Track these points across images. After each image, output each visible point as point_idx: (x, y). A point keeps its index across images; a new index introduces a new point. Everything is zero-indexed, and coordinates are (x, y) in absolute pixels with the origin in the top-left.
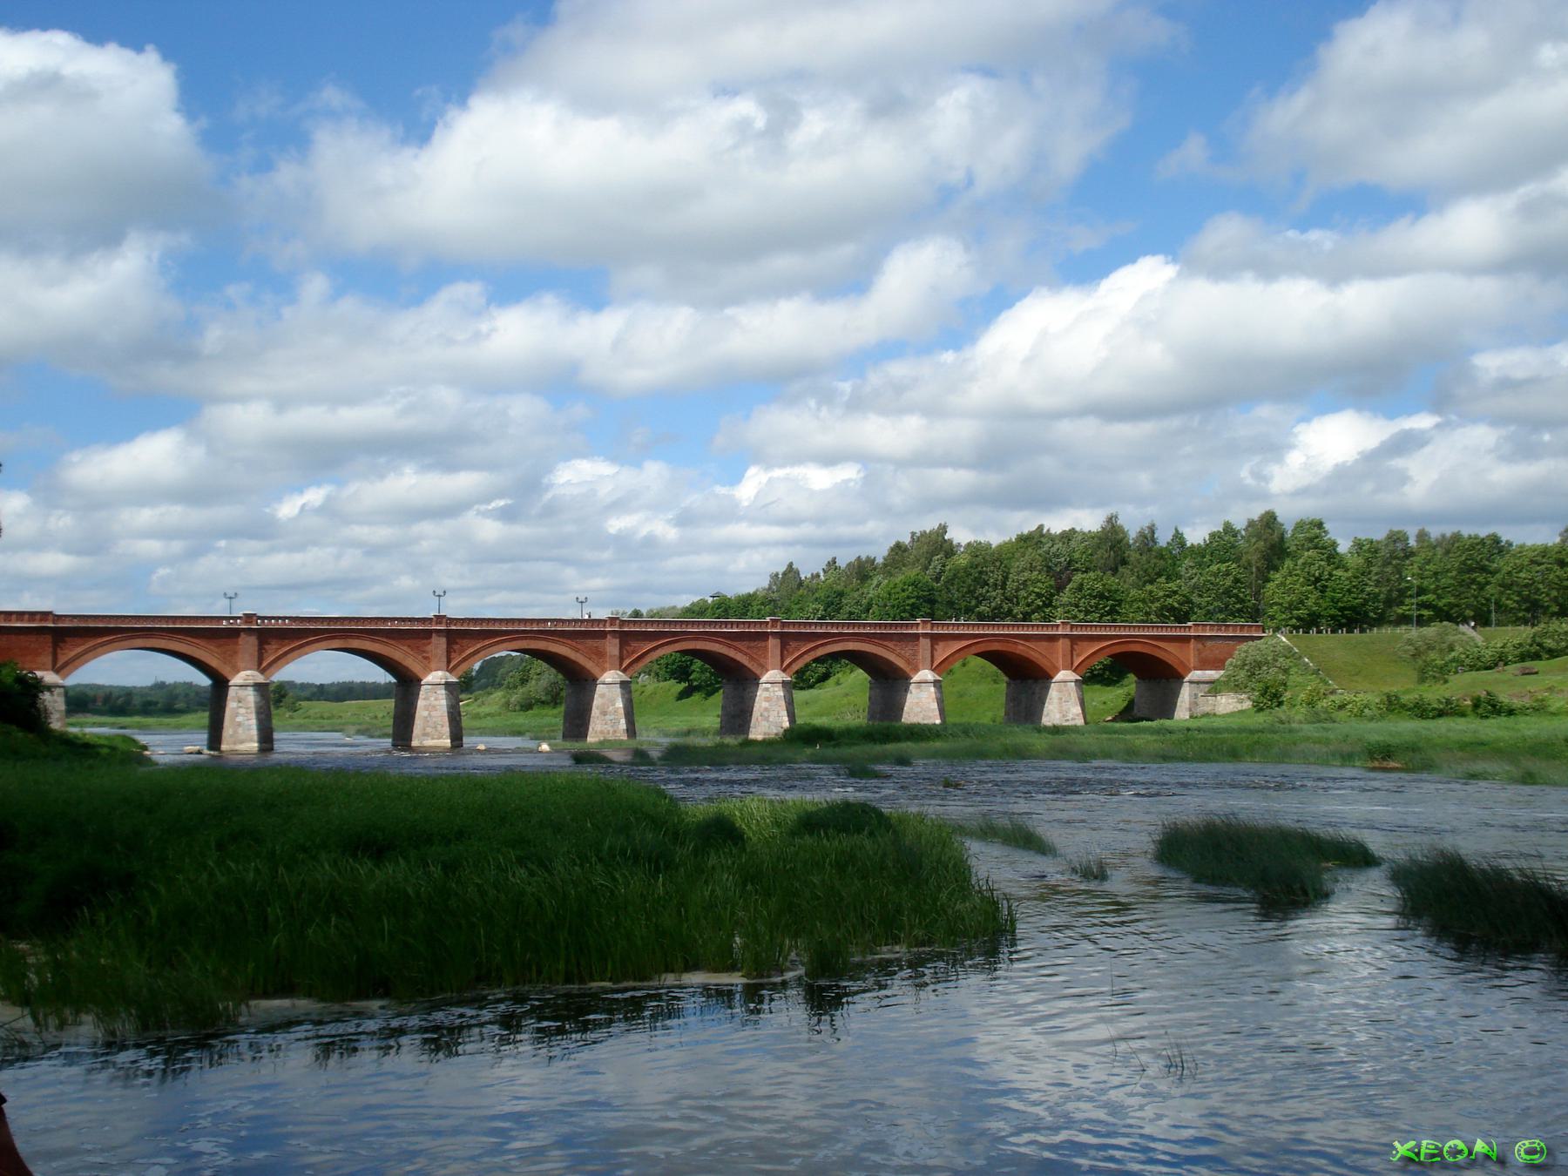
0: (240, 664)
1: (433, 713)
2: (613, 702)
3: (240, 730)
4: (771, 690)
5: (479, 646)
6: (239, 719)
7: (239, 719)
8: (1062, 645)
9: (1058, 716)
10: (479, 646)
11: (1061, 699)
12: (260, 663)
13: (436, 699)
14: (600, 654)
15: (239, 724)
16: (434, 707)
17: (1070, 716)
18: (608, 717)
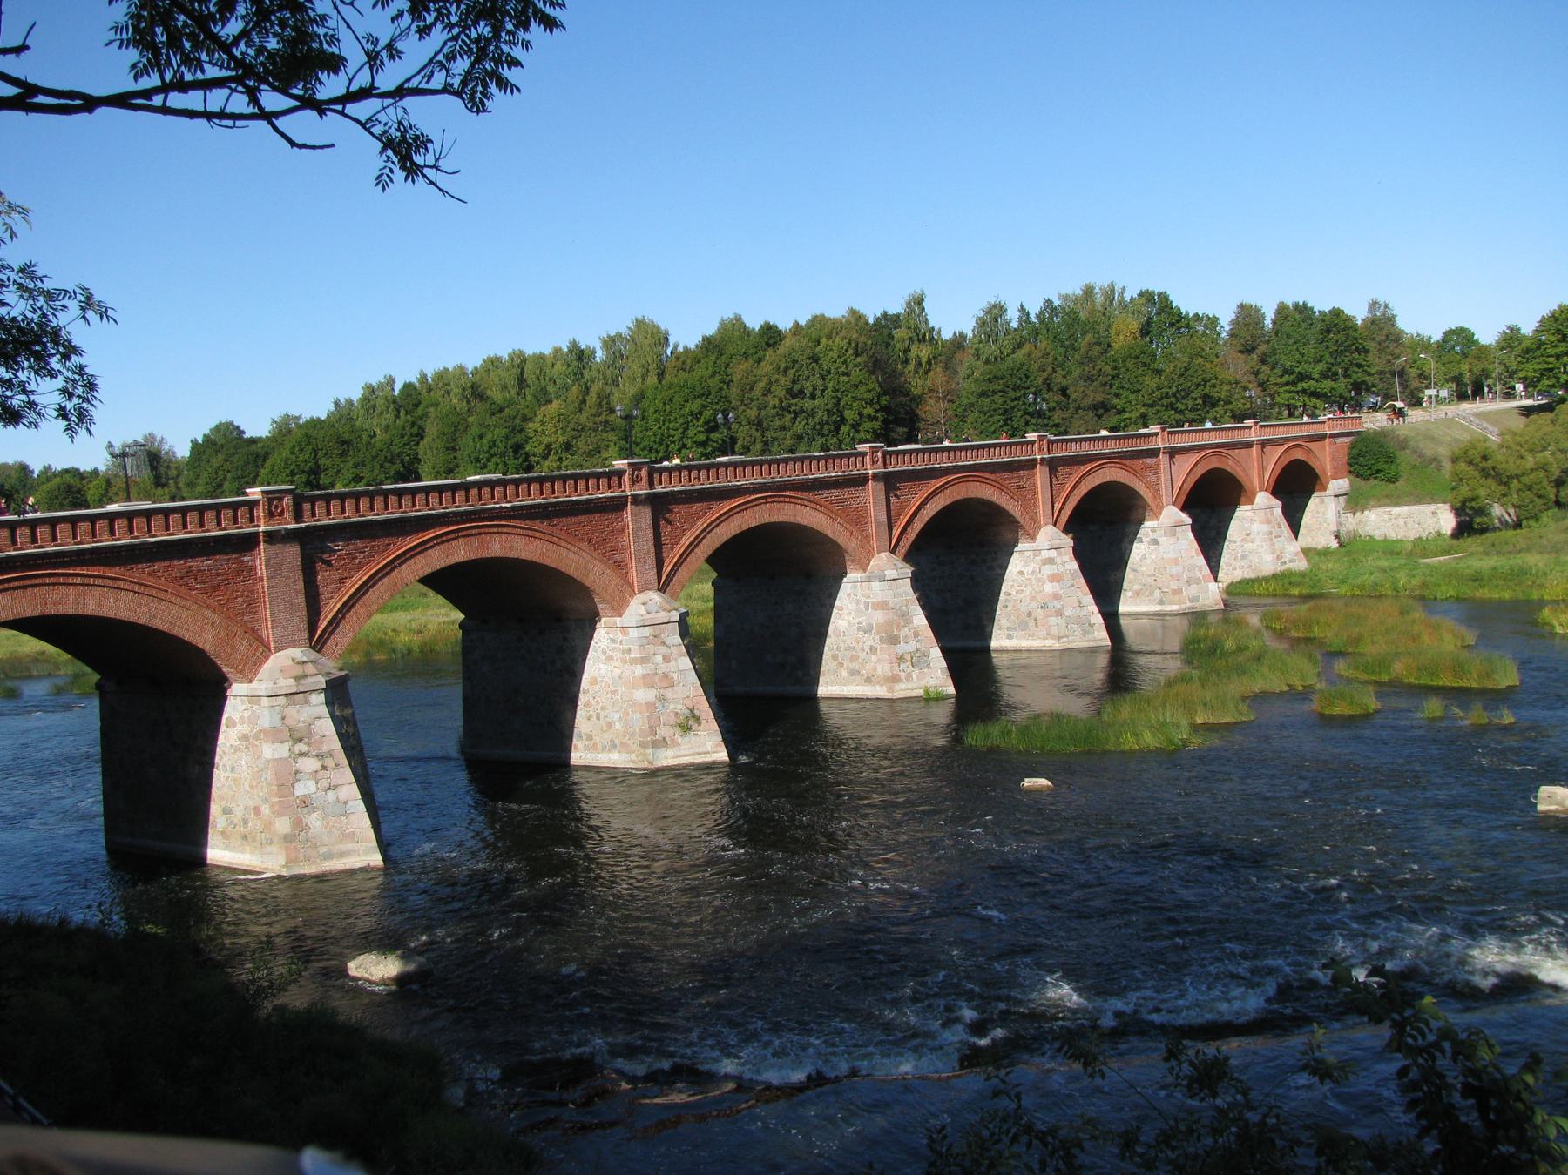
0: (269, 633)
1: (669, 693)
2: (906, 616)
3: (314, 821)
4: (1058, 560)
5: (700, 525)
6: (305, 788)
7: (305, 788)
8: (1255, 450)
9: (1269, 558)
10: (700, 525)
11: (1271, 533)
12: (312, 625)
13: (666, 659)
14: (858, 520)
15: (306, 803)
16: (666, 676)
17: (1287, 557)
18: (902, 648)
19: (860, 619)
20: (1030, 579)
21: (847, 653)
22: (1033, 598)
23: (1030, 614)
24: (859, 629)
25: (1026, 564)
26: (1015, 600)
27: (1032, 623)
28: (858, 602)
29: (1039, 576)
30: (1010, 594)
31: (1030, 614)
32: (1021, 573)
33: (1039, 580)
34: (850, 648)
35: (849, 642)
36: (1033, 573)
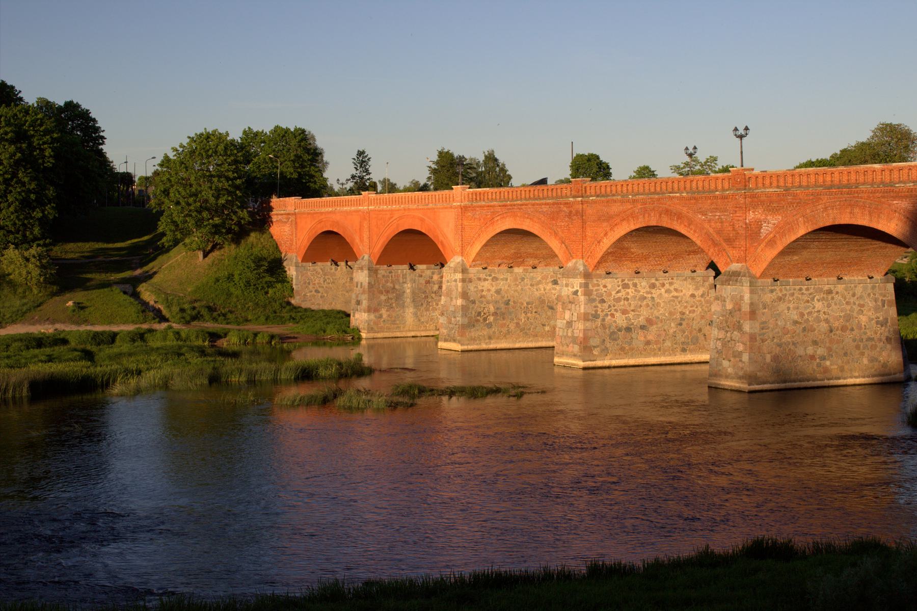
19: (878, 315)
20: (700, 301)
21: (867, 343)
22: (702, 317)
23: (700, 330)
24: (877, 323)
25: (697, 289)
26: (689, 319)
27: (701, 338)
28: (876, 300)
29: (707, 298)
30: (684, 314)
31: (700, 330)
32: (693, 296)
33: (707, 302)
34: (869, 339)
35: (869, 334)
36: (702, 296)
